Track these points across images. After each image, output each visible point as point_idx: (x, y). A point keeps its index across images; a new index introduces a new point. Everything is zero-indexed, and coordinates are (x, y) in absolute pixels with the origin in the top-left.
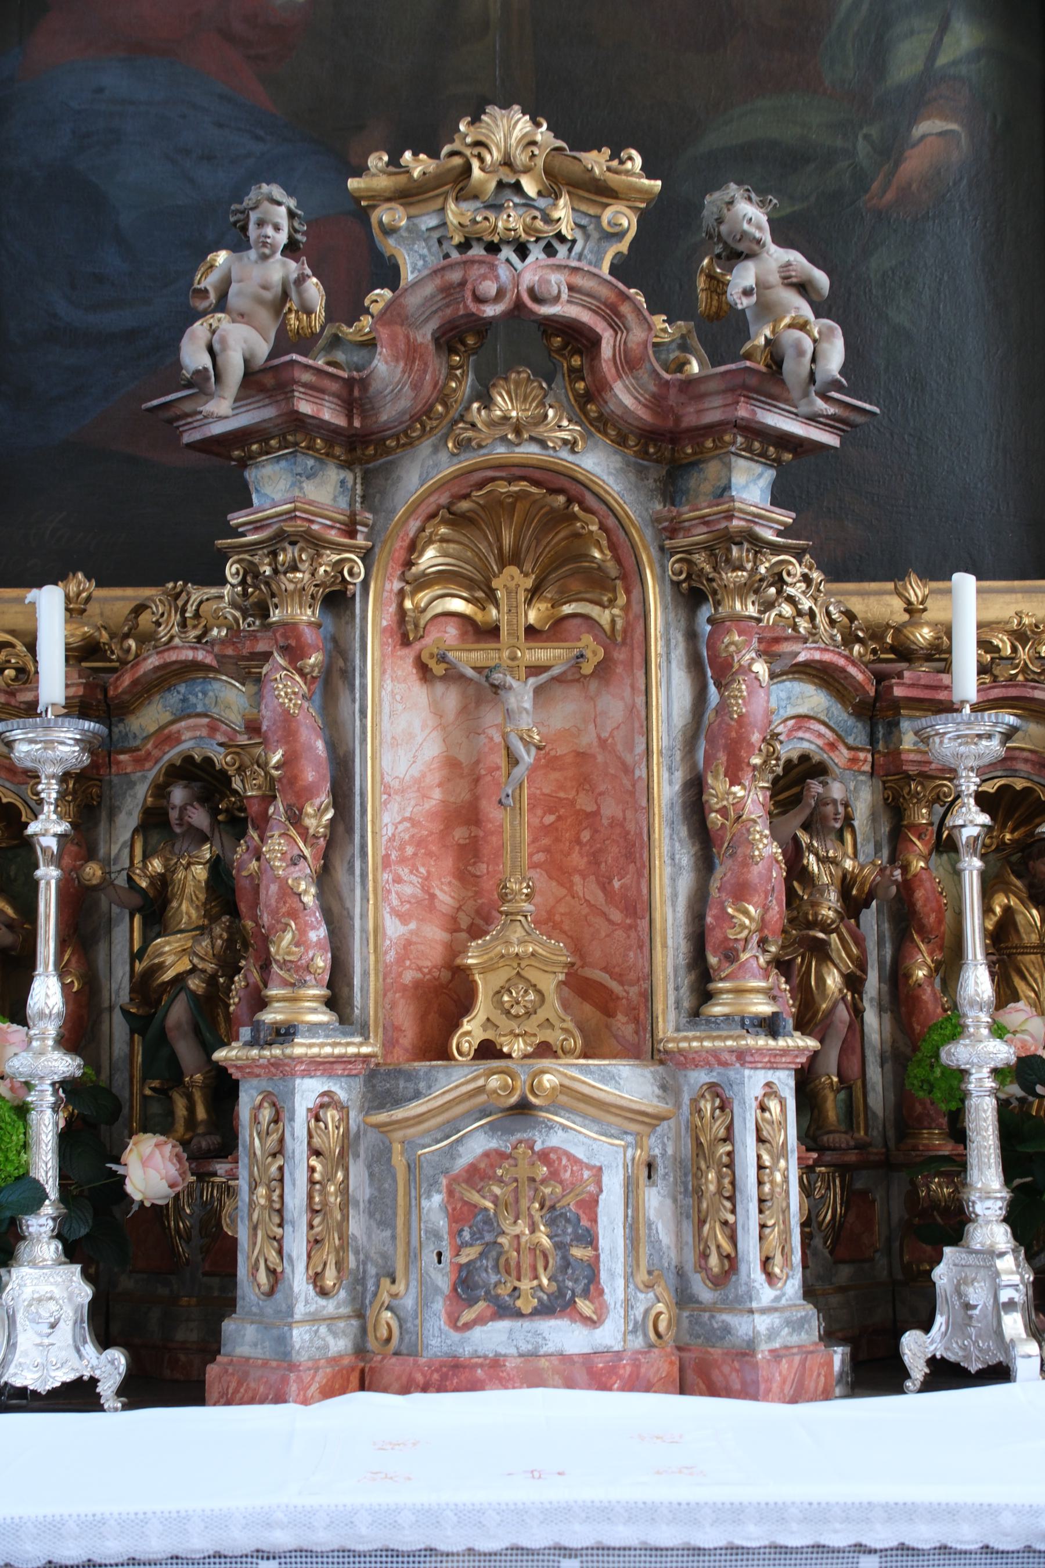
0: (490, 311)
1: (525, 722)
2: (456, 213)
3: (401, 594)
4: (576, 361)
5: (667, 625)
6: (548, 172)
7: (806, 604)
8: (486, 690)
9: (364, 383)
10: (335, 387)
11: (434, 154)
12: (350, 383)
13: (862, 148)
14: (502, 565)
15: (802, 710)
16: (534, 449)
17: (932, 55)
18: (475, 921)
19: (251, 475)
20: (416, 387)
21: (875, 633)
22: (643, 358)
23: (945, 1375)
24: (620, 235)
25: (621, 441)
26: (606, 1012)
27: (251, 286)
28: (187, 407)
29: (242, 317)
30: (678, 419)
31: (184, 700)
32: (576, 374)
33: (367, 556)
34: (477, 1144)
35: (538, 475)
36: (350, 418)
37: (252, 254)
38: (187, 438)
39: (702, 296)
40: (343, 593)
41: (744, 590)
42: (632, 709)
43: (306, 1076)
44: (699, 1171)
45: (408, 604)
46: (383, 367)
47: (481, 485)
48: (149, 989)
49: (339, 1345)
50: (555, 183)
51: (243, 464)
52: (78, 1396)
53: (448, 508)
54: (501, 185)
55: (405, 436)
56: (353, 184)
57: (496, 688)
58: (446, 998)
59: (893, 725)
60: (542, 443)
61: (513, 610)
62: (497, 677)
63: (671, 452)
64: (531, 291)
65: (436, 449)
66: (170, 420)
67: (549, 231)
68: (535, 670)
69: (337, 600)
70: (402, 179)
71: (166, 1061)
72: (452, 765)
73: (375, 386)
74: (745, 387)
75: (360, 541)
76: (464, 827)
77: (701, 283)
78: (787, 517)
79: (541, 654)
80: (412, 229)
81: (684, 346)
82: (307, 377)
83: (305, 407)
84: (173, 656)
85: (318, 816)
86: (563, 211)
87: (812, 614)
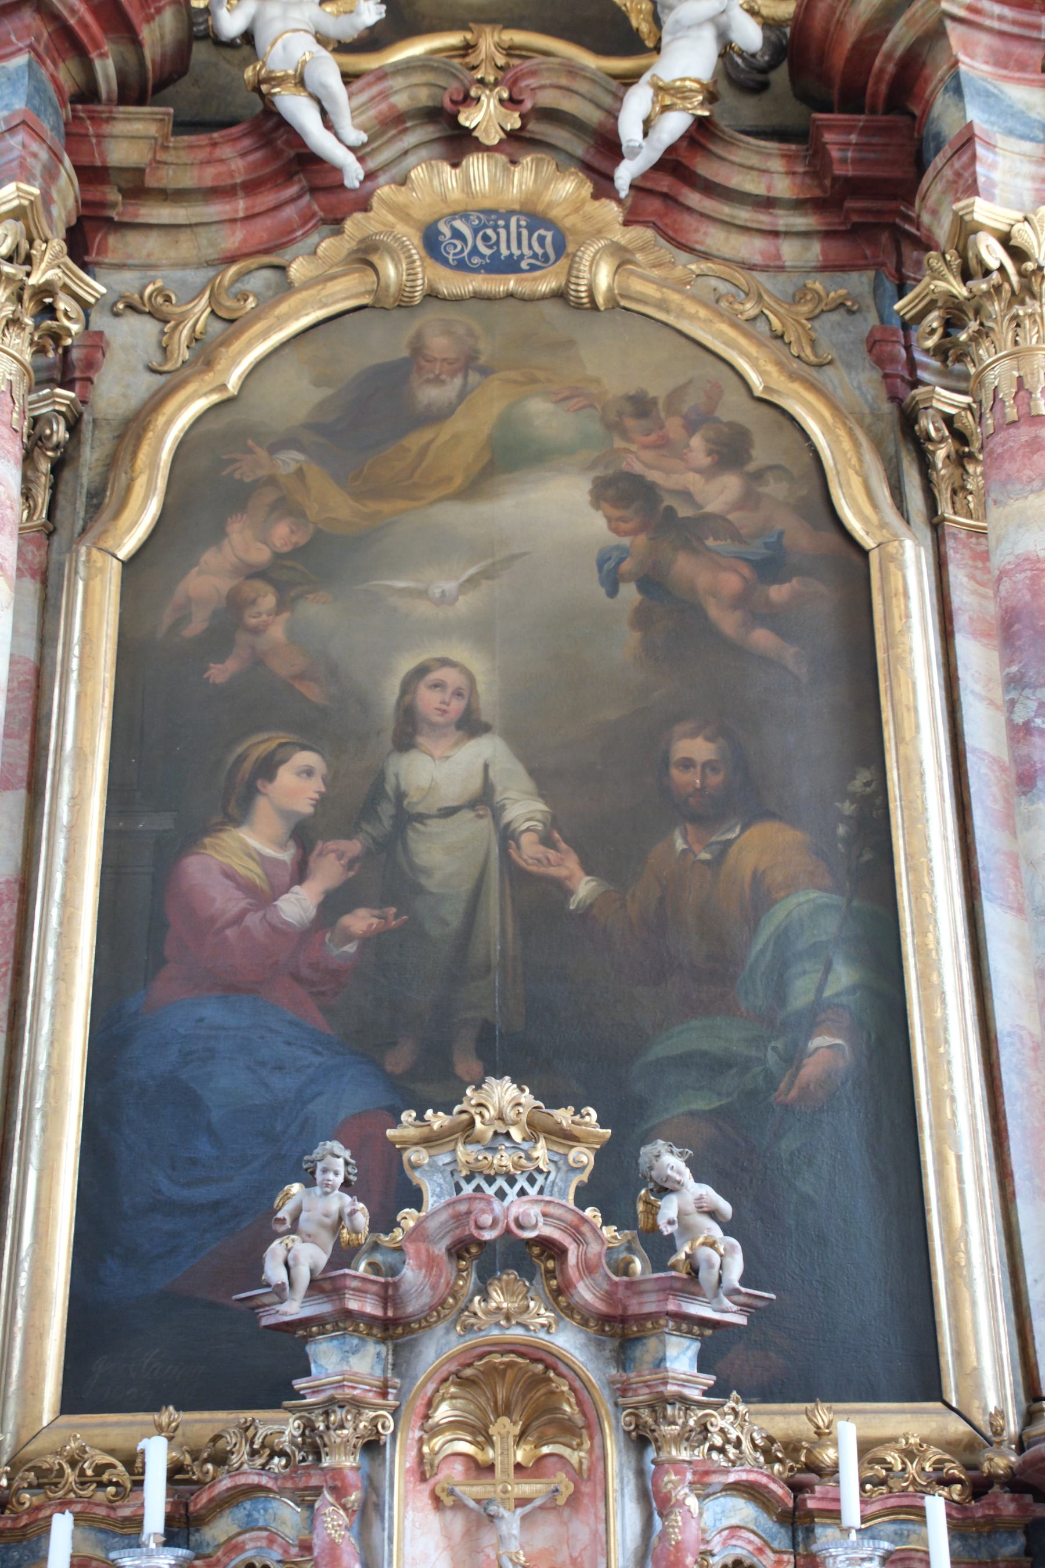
0: (488, 1236)
1: (514, 1546)
2: (465, 1153)
3: (421, 1441)
4: (551, 1264)
5: (621, 1465)
6: (530, 1124)
7: (733, 1434)
8: (484, 1518)
9: (396, 1286)
10: (374, 1288)
11: (449, 1112)
12: (386, 1286)
13: (771, 1058)
14: (497, 1416)
15: (734, 1521)
16: (520, 1331)
17: (820, 989)
19: (310, 1349)
20: (434, 1287)
21: (792, 1447)
22: (598, 1265)
24: (582, 1169)
25: (584, 1323)
27: (317, 1215)
28: (266, 1300)
29: (309, 1238)
30: (625, 1308)
31: (249, 1515)
32: (550, 1274)
33: (395, 1412)
35: (523, 1349)
36: (385, 1309)
37: (318, 1190)
38: (264, 1322)
39: (641, 1216)
40: (377, 1442)
41: (677, 1440)
42: (595, 1534)
45: (426, 1449)
46: (411, 1274)
47: (481, 1357)
50: (535, 1129)
51: (306, 1340)
53: (457, 1374)
54: (496, 1134)
55: (425, 1321)
56: (390, 1132)
57: (492, 1517)
59: (810, 1531)
60: (526, 1327)
61: (505, 1452)
62: (493, 1509)
63: (621, 1331)
64: (517, 1221)
65: (448, 1331)
66: (253, 1308)
67: (531, 1166)
68: (521, 1502)
69: (372, 1447)
70: (426, 1130)
73: (404, 1287)
74: (671, 1289)
75: (391, 1401)
77: (640, 1207)
78: (709, 1380)
79: (527, 1488)
80: (432, 1165)
81: (630, 1249)
82: (355, 1284)
83: (353, 1305)
84: (242, 1480)
86: (541, 1151)
87: (738, 1444)
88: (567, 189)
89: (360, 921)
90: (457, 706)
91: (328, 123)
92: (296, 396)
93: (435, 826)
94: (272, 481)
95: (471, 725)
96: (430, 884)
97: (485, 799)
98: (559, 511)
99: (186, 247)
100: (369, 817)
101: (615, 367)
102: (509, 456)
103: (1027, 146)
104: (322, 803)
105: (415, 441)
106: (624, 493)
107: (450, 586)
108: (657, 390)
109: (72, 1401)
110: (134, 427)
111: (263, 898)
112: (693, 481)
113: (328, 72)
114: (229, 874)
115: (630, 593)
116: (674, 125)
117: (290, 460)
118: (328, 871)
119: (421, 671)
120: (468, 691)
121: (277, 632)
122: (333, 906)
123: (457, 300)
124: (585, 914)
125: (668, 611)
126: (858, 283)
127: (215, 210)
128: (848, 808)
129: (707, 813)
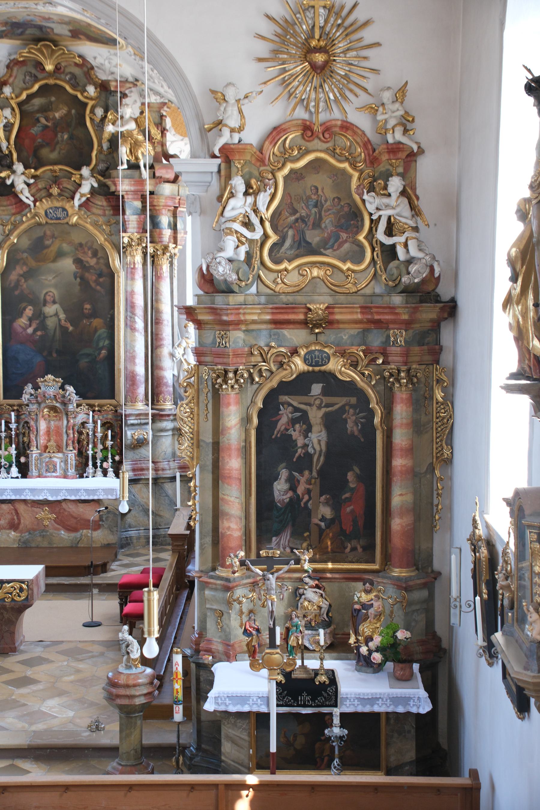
2: (46, 383)
8: (49, 422)
18: (49, 441)
23: (87, 477)
26: (59, 449)
34: (47, 460)
43: (34, 453)
48: (24, 443)
49: (37, 474)
50: (54, 380)
52: (17, 478)
58: (46, 447)
63: (64, 404)
69: (37, 415)
72: (47, 427)
76: (48, 433)
85: (35, 433)
89: (39, 333)
90: (52, 299)
91: (27, 198)
92: (26, 243)
93: (49, 318)
94: (22, 259)
95: (54, 302)
96: (49, 328)
97: (56, 315)
98: (67, 265)
99: (6, 213)
100: (39, 317)
101: (77, 237)
102: (60, 255)
103: (135, 217)
104: (33, 315)
105: (45, 251)
106: (78, 262)
107: (51, 278)
108: (83, 242)
111: (25, 329)
112: (89, 260)
113: (26, 193)
114: (20, 326)
115: (78, 279)
116: (84, 199)
117: (25, 255)
118: (34, 325)
119: (47, 293)
120: (54, 297)
121: (25, 286)
122: (35, 331)
123: (51, 224)
124: (71, 333)
125: (84, 283)
127: (10, 207)
128: (109, 316)
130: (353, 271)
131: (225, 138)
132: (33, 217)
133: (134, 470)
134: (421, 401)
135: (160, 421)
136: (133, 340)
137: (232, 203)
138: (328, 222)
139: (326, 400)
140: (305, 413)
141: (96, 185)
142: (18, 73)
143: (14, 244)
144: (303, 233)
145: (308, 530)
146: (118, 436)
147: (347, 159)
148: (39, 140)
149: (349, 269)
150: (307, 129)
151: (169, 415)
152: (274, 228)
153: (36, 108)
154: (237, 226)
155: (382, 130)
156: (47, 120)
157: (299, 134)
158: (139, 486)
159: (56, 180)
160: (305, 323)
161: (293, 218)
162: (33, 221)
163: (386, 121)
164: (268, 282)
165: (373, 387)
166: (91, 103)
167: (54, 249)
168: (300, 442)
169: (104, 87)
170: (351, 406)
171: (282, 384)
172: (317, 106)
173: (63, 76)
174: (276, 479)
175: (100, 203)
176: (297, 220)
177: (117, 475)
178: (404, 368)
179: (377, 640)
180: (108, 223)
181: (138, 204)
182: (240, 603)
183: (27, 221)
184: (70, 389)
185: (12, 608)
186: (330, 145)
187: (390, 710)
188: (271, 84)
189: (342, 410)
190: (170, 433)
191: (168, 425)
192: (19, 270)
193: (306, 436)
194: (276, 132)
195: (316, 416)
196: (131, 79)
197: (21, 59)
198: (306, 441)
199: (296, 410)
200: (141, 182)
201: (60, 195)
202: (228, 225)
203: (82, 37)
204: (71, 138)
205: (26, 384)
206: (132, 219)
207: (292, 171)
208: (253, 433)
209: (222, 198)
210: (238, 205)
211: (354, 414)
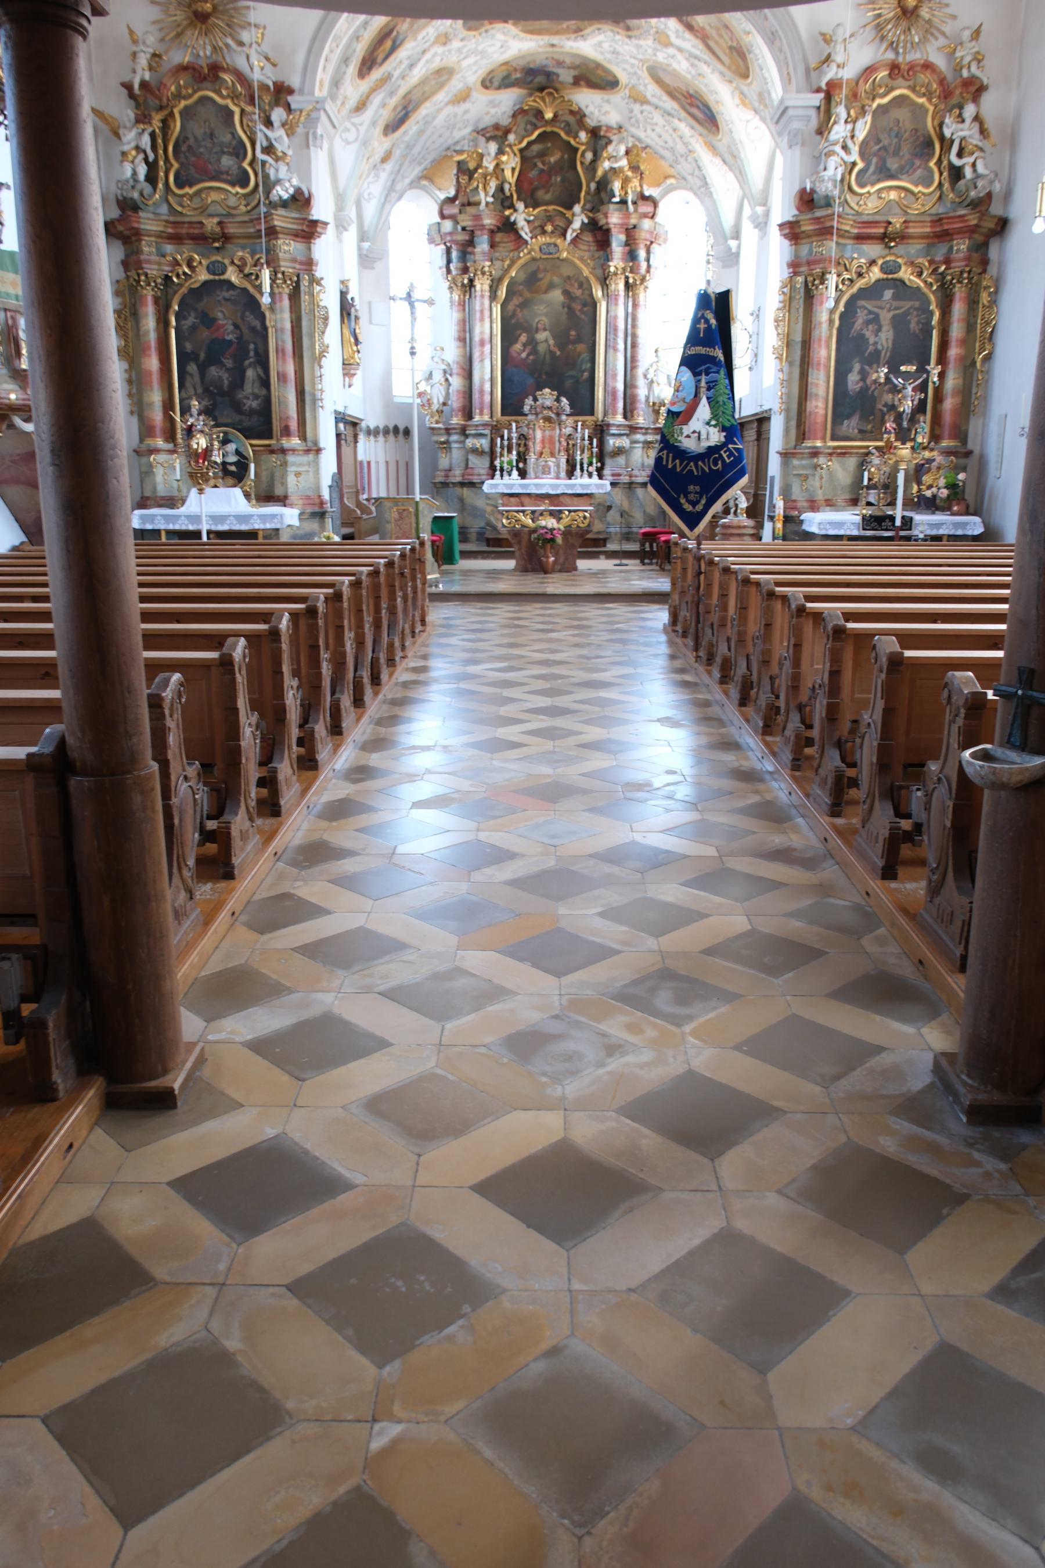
18: (544, 448)
26: (552, 455)
43: (532, 458)
44: (558, 466)
58: (541, 454)
63: (558, 414)
71: (522, 457)
76: (543, 441)
88: (559, 241)
89: (531, 357)
92: (522, 276)
95: (545, 330)
97: (546, 341)
100: (532, 342)
101: (566, 271)
102: (551, 287)
106: (566, 293)
109: (503, 414)
110: (500, 280)
111: (519, 354)
112: (575, 291)
113: (527, 229)
116: (575, 234)
117: (521, 287)
118: (527, 351)
122: (528, 355)
126: (601, 253)
129: (574, 342)
130: (923, 194)
131: (831, 73)
132: (529, 253)
133: (613, 475)
134: (972, 303)
135: (635, 433)
136: (615, 359)
137: (836, 128)
138: (905, 151)
139: (895, 304)
140: (877, 315)
141: (586, 221)
142: (521, 120)
143: (512, 278)
144: (884, 161)
145: (872, 414)
146: (601, 444)
147: (924, 95)
148: (536, 183)
149: (919, 192)
150: (894, 68)
151: (641, 428)
152: (862, 154)
153: (534, 153)
154: (838, 149)
155: (958, 68)
156: (544, 163)
157: (886, 73)
158: (616, 489)
159: (550, 219)
160: (884, 238)
161: (877, 147)
162: (529, 256)
163: (962, 58)
164: (853, 205)
165: (934, 293)
166: (582, 148)
167: (545, 282)
168: (872, 340)
169: (595, 133)
170: (917, 309)
171: (860, 289)
172: (904, 47)
173: (558, 124)
174: (850, 371)
175: (586, 239)
176: (880, 149)
177: (600, 477)
178: (967, 269)
179: (942, 482)
180: (592, 258)
181: (623, 237)
182: (822, 469)
183: (525, 255)
184: (564, 400)
185: (577, 533)
186: (910, 83)
187: (951, 533)
188: (868, 28)
189: (907, 313)
190: (640, 445)
191: (639, 437)
192: (516, 301)
193: (877, 335)
194: (869, 70)
195: (886, 317)
196: (615, 126)
197: (526, 108)
198: (877, 339)
199: (870, 312)
200: (627, 215)
201: (552, 232)
202: (831, 148)
203: (582, 83)
204: (563, 180)
205: (526, 397)
206: (617, 248)
207: (879, 106)
208: (835, 332)
209: (822, 130)
210: (839, 131)
211: (918, 316)
